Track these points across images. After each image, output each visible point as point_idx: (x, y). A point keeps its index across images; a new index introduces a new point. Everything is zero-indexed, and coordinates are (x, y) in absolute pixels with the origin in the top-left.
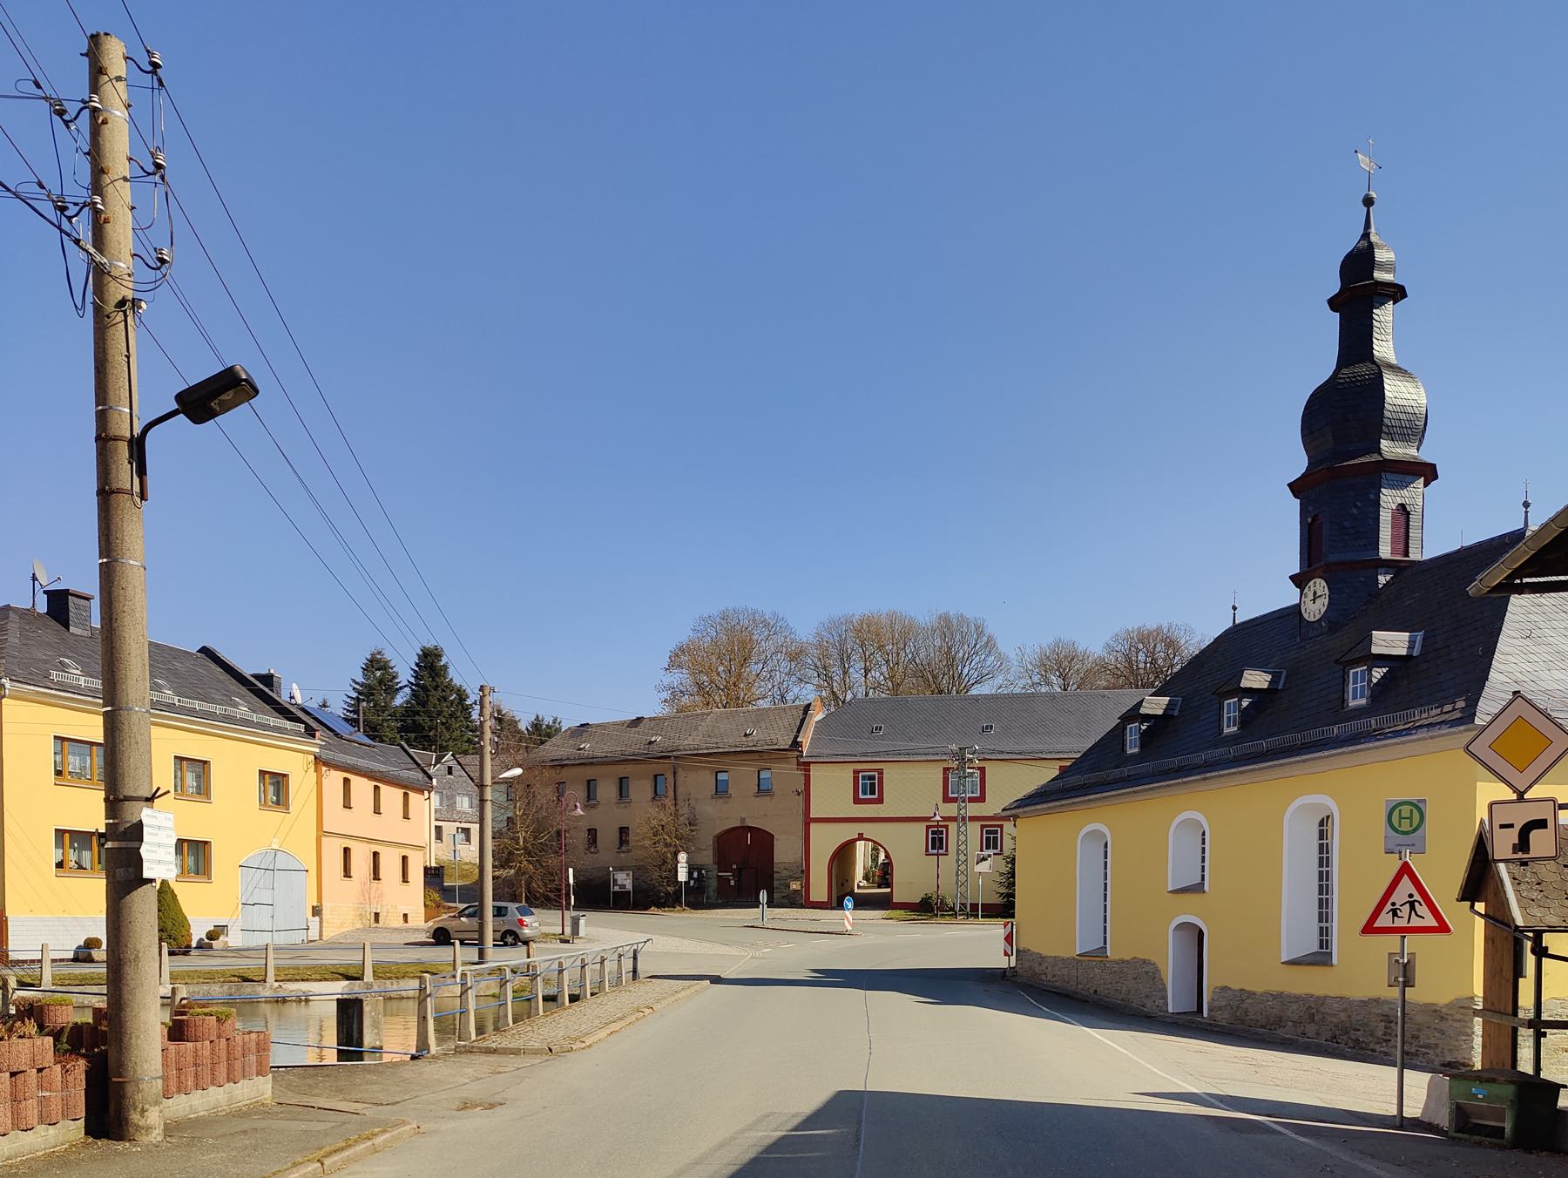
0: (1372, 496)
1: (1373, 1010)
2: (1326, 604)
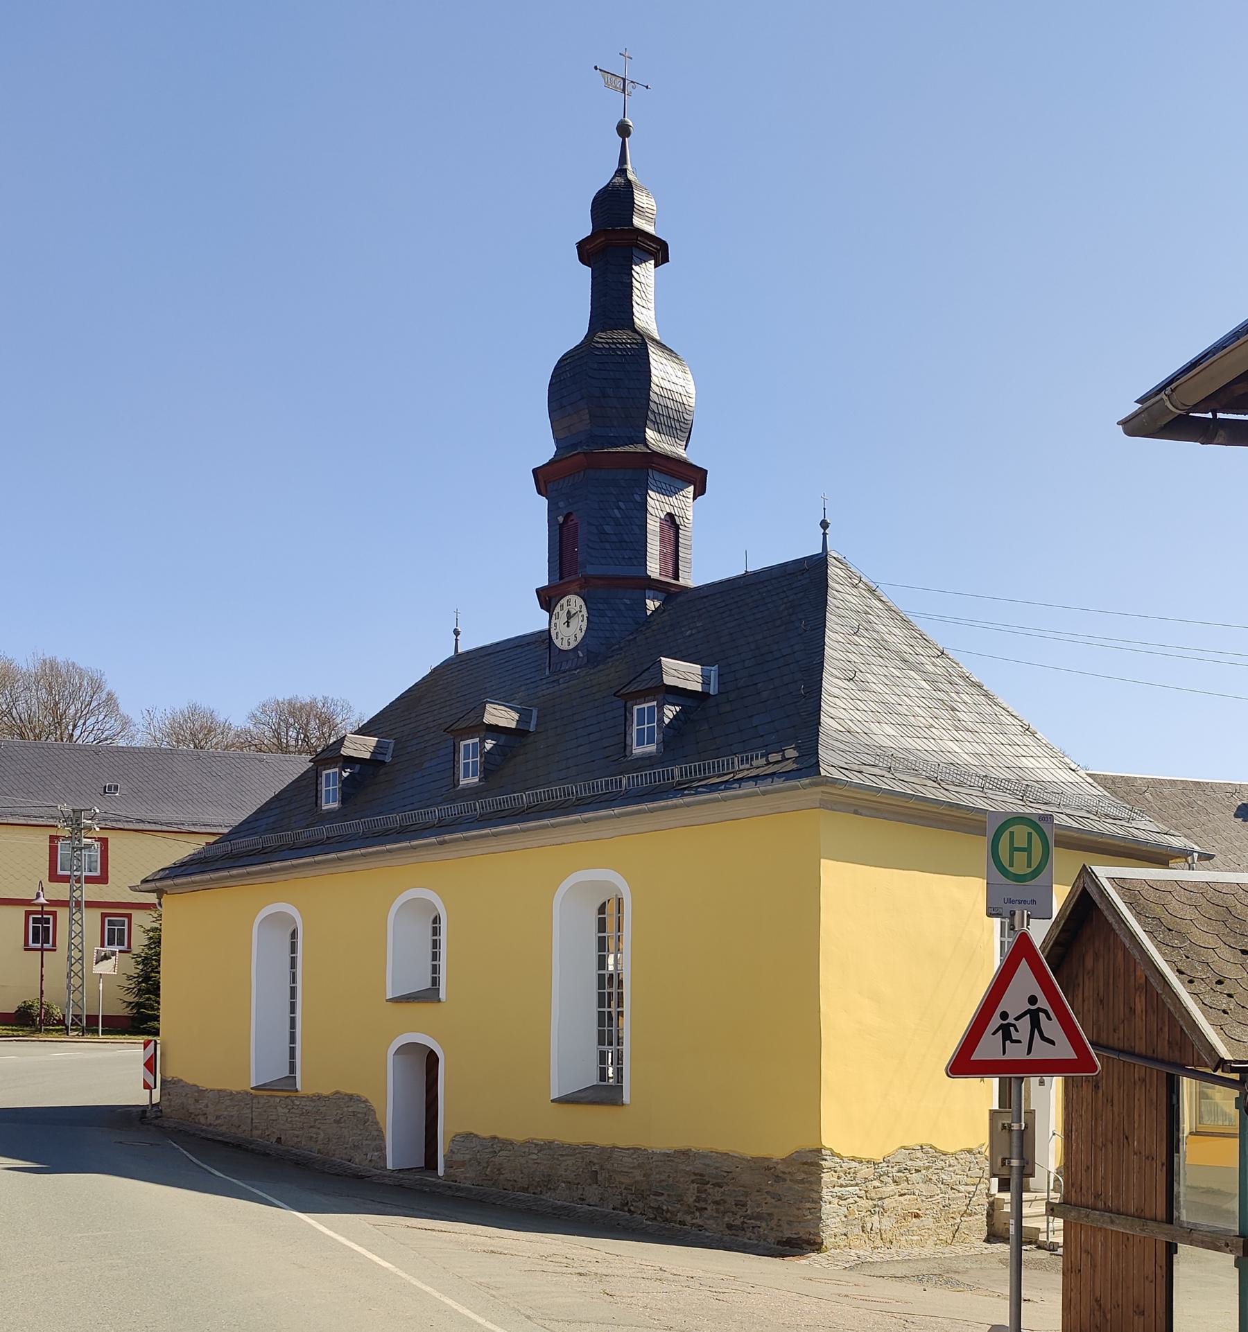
0: (637, 498)
1: (682, 1167)
2: (584, 628)
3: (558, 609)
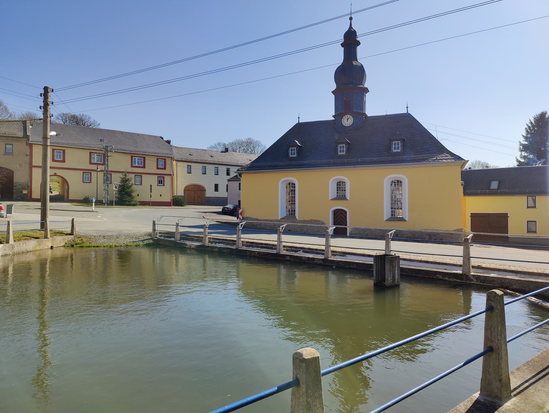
3: (344, 117)
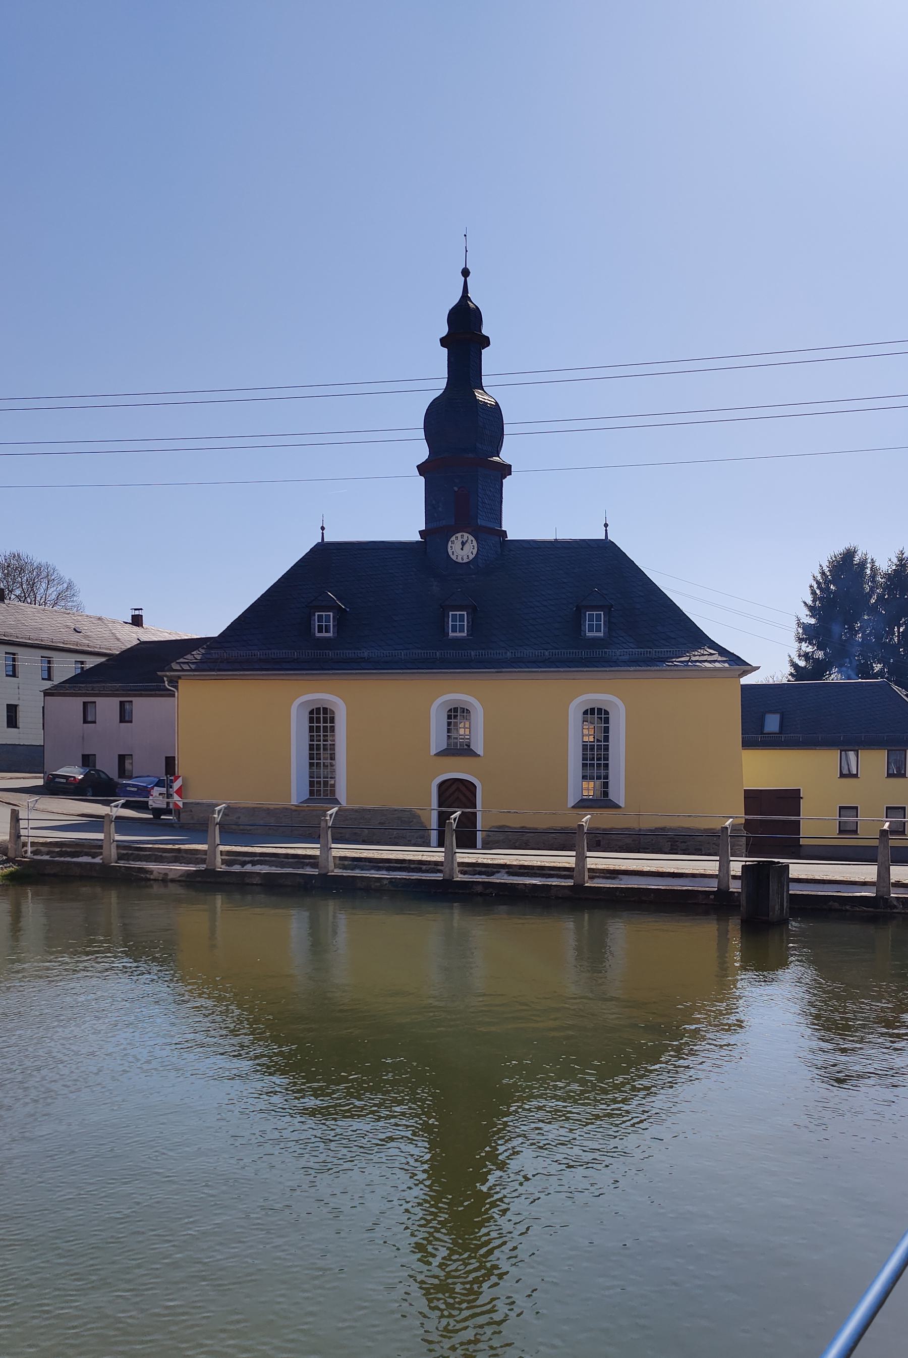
3: (453, 538)
